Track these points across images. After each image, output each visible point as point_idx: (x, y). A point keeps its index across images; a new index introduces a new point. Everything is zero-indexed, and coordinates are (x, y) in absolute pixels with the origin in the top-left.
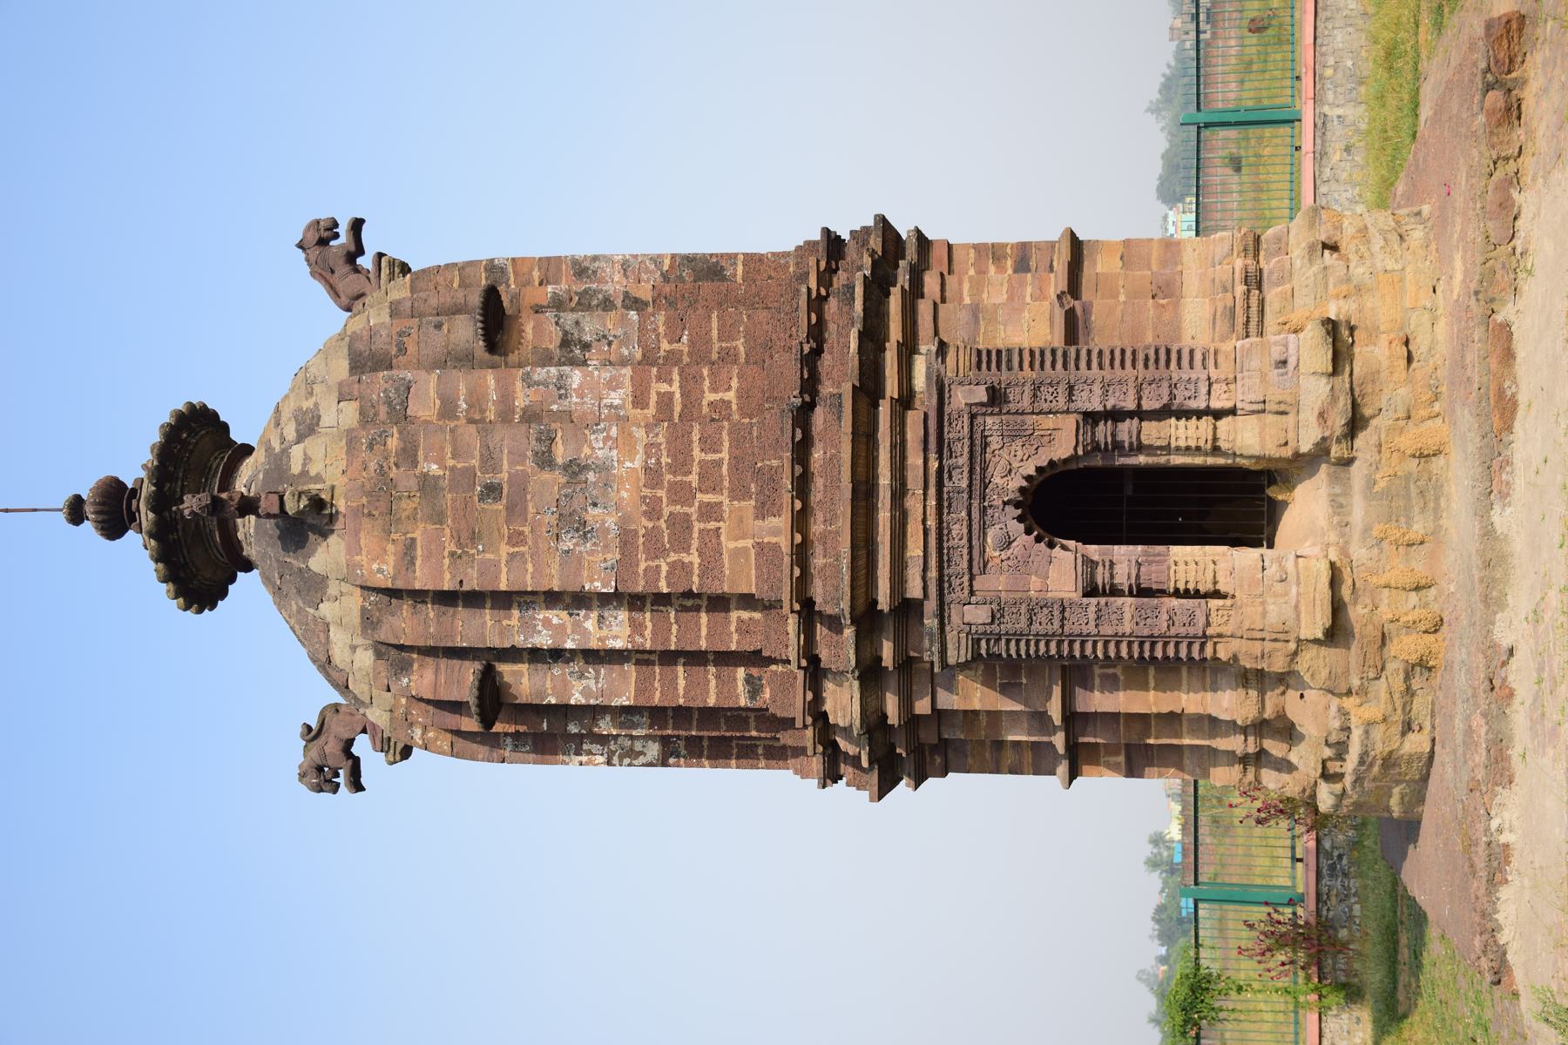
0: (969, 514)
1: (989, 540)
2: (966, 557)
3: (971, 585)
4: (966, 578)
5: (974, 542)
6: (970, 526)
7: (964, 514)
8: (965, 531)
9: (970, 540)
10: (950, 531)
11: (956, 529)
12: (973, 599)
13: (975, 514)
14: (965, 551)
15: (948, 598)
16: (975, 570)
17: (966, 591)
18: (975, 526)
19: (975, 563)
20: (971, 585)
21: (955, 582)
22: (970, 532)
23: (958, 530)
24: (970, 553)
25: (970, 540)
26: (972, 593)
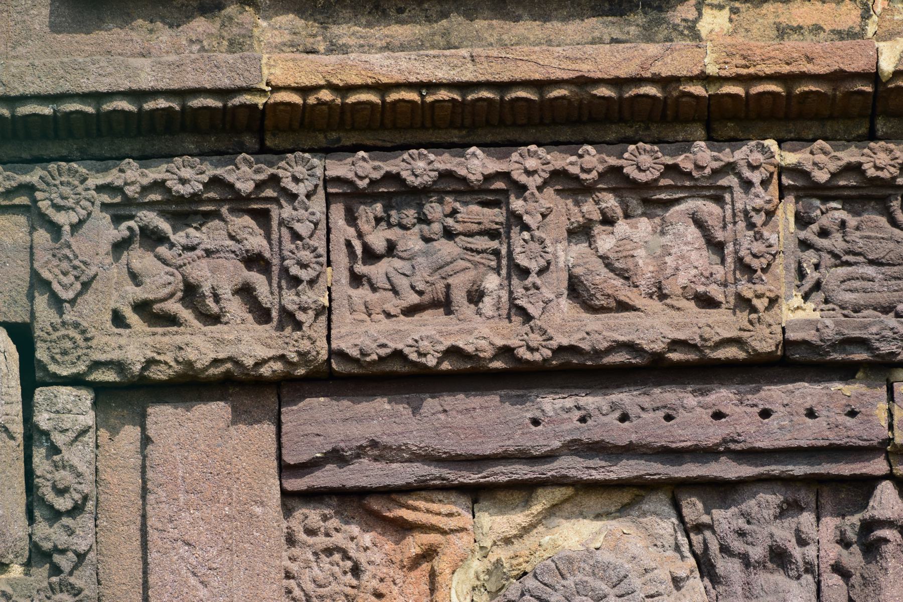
0: (795, 361)
1: (574, 533)
2: (428, 338)
3: (189, 386)
4: (251, 344)
5: (558, 411)
6: (697, 368)
7: (799, 315)
8: (654, 327)
9: (574, 370)
10: (646, 198)
11: (664, 247)
12: (68, 409)
13: (797, 414)
14: (481, 332)
15: (74, 188)
16: (320, 421)
17: (136, 346)
18: (692, 415)
19: (379, 417)
20: (189, 386)
21: (214, 252)
22: (652, 369)
23: (660, 267)
24: (467, 374)
25: (574, 370)
26: (127, 394)
